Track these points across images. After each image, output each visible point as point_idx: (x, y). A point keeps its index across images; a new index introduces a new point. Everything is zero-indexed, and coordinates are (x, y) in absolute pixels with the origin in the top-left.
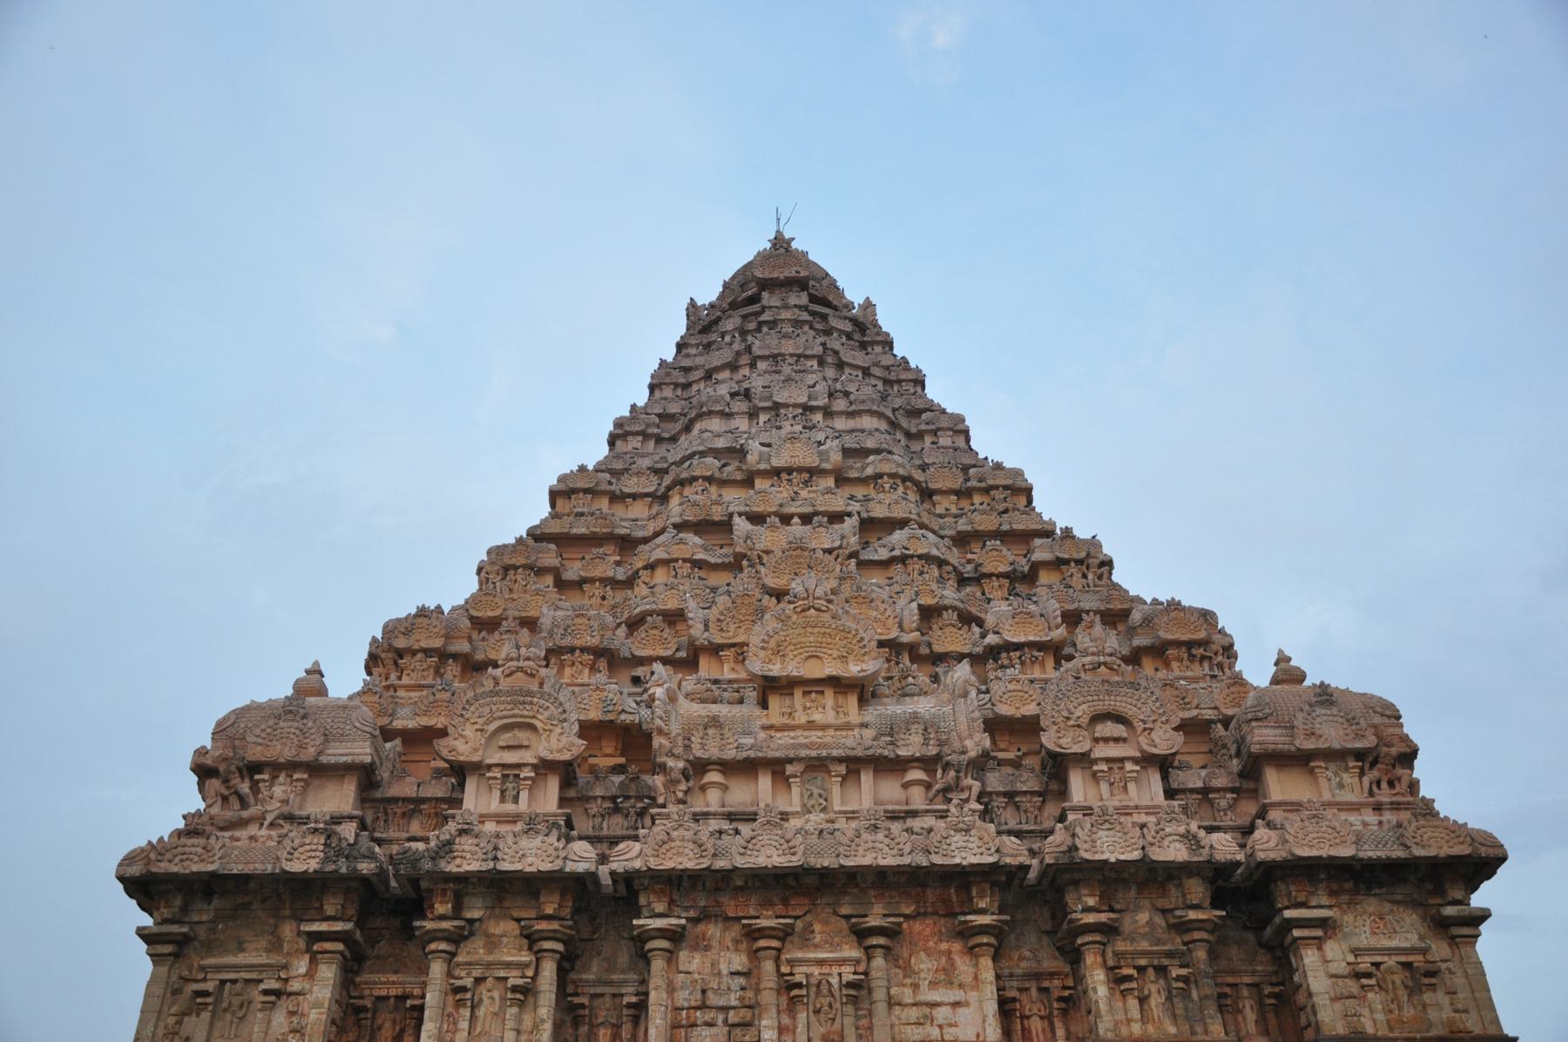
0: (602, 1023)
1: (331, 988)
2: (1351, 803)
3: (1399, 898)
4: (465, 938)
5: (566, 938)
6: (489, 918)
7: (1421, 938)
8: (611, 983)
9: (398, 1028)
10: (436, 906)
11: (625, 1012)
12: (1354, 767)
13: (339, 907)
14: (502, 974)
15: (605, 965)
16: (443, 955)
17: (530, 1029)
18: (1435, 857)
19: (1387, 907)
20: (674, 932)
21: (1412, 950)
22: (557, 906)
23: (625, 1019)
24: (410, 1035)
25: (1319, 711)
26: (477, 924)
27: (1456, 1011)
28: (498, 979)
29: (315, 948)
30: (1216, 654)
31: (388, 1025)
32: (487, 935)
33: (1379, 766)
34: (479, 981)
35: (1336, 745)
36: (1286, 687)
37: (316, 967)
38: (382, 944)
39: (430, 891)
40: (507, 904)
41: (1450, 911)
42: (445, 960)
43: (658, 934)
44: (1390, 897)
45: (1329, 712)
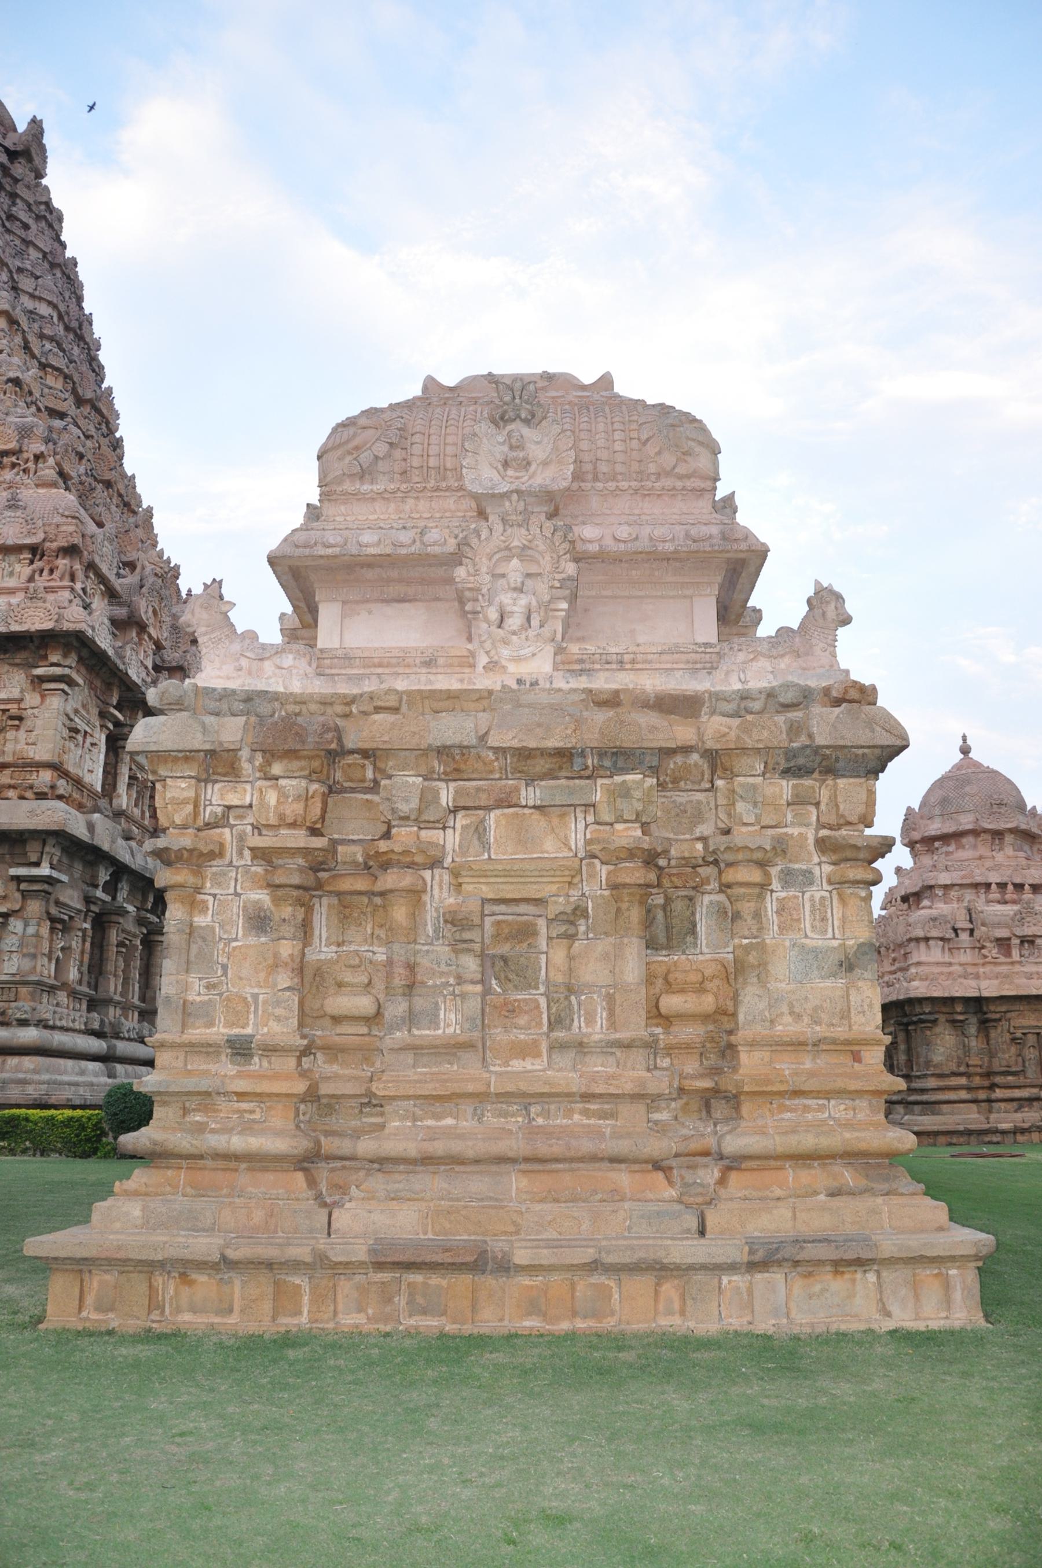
2: (8, 588)
3: (18, 661)
7: (22, 692)
12: (24, 559)
18: (27, 631)
19: (6, 667)
21: (9, 701)
25: (7, 513)
27: (27, 744)
30: (27, 461)
33: (45, 558)
35: (10, 542)
36: (41, 491)
41: (39, 671)
44: (11, 661)
45: (13, 514)
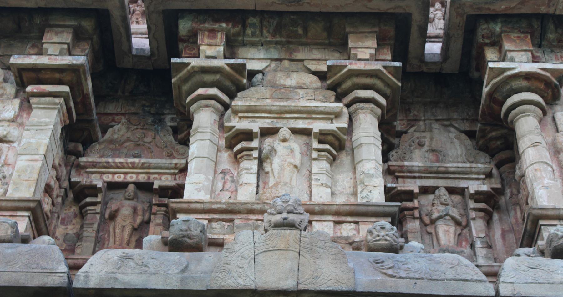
0: (440, 218)
1: (49, 133)
4: (241, 88)
5: (388, 91)
6: (275, 70)
8: (445, 174)
9: (139, 220)
10: (202, 48)
11: (472, 204)
13: (65, 46)
14: (301, 124)
15: (431, 156)
16: (213, 102)
17: (351, 190)
20: (547, 83)
22: (373, 51)
23: (473, 214)
24: (158, 225)
26: (259, 76)
28: (295, 131)
29: (29, 89)
31: (126, 210)
32: (274, 86)
34: (267, 132)
37: (29, 114)
38: (116, 127)
39: (193, 37)
40: (299, 56)
42: (216, 109)
43: (524, 83)
